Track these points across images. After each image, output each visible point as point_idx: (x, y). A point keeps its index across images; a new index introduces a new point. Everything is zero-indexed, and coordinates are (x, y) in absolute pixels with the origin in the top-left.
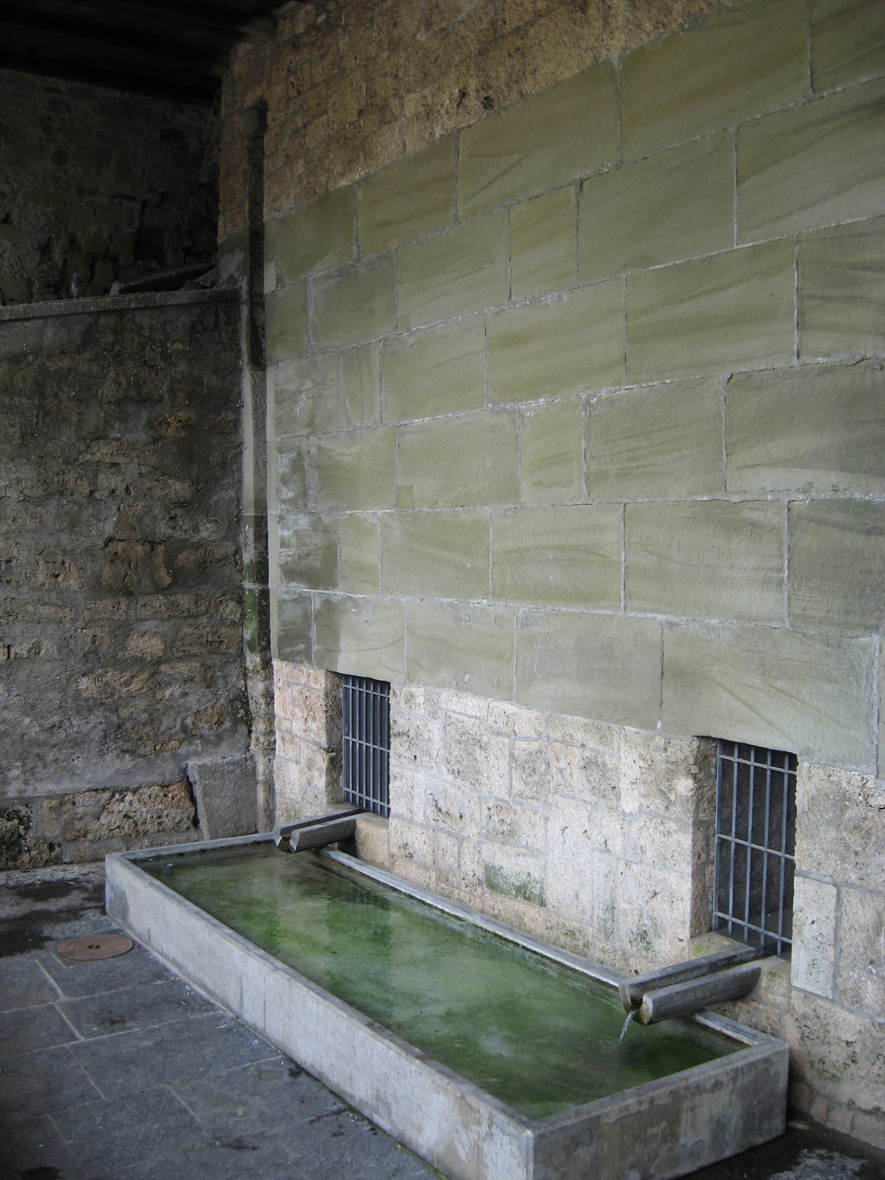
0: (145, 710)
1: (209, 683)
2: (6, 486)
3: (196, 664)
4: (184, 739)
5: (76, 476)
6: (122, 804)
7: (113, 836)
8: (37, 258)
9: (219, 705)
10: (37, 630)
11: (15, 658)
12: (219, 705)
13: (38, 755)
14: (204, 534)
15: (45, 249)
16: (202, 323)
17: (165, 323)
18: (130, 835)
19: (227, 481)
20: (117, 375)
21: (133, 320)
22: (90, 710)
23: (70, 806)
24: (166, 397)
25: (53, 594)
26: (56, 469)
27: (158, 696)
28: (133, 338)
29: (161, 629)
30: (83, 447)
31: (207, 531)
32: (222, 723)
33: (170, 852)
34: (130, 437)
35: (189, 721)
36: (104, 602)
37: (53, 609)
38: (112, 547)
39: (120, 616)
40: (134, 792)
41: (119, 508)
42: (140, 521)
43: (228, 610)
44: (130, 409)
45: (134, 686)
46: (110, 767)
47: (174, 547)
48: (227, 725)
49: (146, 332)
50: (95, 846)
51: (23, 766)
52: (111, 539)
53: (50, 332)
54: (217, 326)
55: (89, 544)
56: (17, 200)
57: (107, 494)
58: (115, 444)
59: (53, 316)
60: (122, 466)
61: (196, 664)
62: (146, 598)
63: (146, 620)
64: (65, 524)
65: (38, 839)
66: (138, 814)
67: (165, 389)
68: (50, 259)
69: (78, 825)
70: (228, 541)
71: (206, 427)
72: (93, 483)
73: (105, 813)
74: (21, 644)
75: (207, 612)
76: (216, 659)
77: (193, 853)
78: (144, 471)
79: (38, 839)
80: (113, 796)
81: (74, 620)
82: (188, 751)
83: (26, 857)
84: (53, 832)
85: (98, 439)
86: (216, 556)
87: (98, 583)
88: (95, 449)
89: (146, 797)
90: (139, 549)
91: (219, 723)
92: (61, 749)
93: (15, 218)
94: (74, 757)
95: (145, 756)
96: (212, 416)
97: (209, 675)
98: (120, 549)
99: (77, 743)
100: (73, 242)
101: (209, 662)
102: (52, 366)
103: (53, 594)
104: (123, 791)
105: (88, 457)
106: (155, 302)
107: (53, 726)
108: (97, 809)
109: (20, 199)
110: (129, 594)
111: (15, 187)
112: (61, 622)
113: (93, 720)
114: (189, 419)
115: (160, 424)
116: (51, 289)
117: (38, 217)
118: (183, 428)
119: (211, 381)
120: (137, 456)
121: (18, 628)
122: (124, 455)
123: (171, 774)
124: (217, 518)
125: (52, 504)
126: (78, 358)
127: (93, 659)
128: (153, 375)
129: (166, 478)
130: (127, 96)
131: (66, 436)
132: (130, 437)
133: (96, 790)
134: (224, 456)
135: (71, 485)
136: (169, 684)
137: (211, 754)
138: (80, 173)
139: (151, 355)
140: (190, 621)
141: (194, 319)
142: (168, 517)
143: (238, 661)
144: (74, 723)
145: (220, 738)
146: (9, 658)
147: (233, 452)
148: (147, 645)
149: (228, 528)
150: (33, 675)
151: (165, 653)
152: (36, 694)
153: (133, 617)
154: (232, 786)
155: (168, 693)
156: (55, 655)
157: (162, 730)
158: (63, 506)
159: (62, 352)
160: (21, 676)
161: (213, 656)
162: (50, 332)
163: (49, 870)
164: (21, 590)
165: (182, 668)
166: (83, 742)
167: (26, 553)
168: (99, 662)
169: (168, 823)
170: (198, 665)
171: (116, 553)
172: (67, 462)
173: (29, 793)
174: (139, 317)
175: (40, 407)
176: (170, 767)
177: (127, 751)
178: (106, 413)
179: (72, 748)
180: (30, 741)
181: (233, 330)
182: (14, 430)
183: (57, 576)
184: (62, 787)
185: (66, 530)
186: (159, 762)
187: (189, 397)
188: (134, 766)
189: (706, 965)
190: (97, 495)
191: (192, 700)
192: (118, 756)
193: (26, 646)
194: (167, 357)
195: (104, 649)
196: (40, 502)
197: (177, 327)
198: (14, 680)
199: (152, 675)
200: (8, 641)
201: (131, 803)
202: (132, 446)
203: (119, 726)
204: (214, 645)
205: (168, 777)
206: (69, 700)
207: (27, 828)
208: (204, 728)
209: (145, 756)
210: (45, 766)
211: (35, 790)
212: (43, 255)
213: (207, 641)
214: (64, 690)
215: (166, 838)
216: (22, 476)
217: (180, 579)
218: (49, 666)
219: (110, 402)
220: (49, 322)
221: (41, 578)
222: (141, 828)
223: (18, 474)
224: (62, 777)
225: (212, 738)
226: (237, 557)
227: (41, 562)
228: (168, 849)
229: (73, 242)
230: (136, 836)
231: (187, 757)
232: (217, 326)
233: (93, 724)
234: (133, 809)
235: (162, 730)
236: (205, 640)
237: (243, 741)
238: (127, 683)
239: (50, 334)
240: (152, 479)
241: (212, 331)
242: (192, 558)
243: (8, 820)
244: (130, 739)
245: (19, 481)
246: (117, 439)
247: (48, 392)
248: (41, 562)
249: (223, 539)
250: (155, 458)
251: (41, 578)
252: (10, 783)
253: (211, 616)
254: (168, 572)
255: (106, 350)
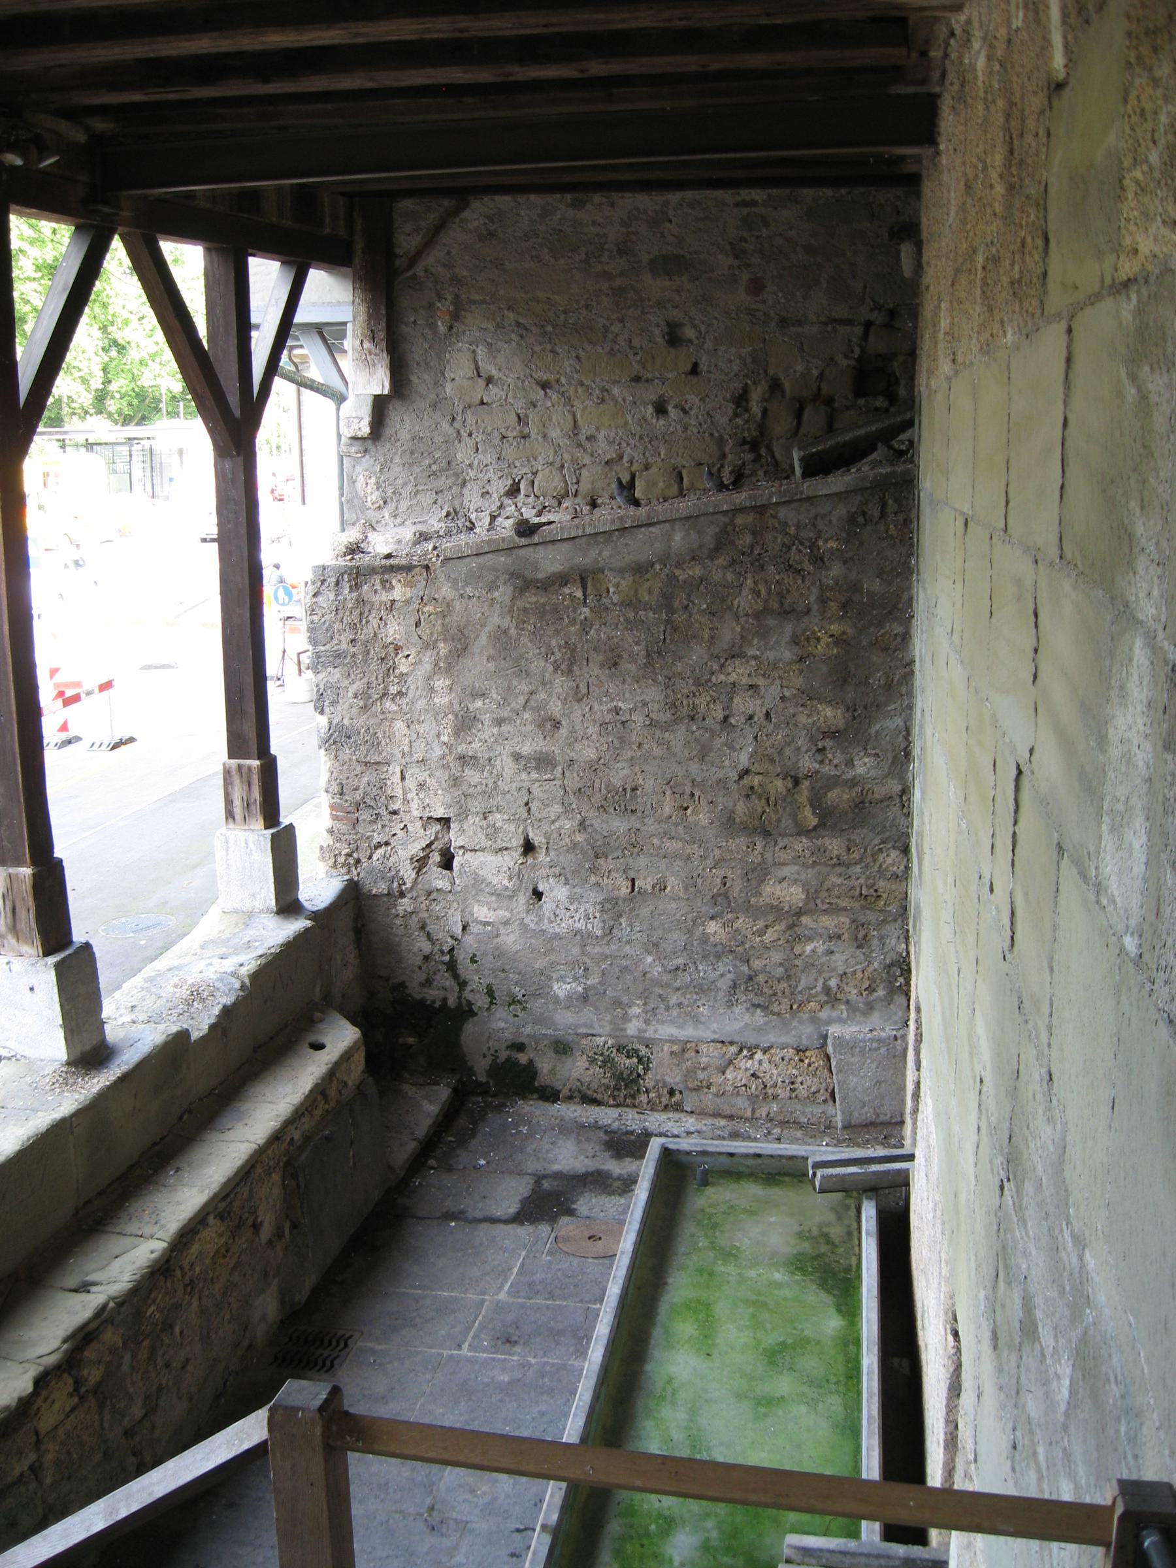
0: (781, 965)
1: (862, 943)
2: (630, 710)
3: (845, 919)
4: (827, 1002)
5: (708, 699)
6: (750, 1062)
7: (738, 1094)
8: (730, 412)
9: (871, 969)
10: (663, 864)
11: (639, 892)
12: (871, 969)
13: (660, 996)
14: (860, 770)
15: (741, 400)
16: (864, 514)
17: (816, 517)
18: (757, 1096)
19: (893, 707)
20: (755, 583)
21: (774, 517)
22: (718, 957)
23: (693, 1054)
24: (815, 607)
25: (680, 828)
26: (686, 691)
27: (797, 950)
28: (776, 538)
29: (803, 876)
30: (716, 667)
31: (864, 766)
32: (874, 990)
33: (718, 1150)
34: (771, 655)
35: (833, 983)
36: (737, 841)
37: (680, 844)
38: (746, 781)
39: (754, 857)
40: (765, 1051)
41: (756, 737)
42: (780, 752)
43: (889, 861)
44: (771, 622)
45: (769, 937)
46: (738, 1021)
47: (821, 787)
48: (881, 993)
49: (792, 530)
50: (718, 1101)
51: (645, 1004)
52: (747, 772)
53: (678, 537)
54: (883, 514)
55: (721, 776)
56: (706, 346)
57: (743, 719)
58: (753, 663)
59: (680, 519)
60: (762, 688)
61: (845, 919)
62: (786, 840)
63: (784, 864)
64: (695, 753)
65: (657, 1082)
66: (768, 1075)
67: (812, 599)
68: (747, 410)
69: (701, 1075)
70: (892, 778)
71: (864, 643)
72: (728, 707)
73: (731, 1068)
74: (645, 878)
75: (861, 860)
76: (872, 917)
77: (746, 1156)
78: (787, 694)
79: (657, 1082)
80: (741, 1050)
81: (703, 858)
82: (830, 1017)
83: (643, 1098)
84: (674, 1078)
85: (733, 657)
86: (876, 796)
87: (731, 820)
88: (730, 669)
89: (777, 1059)
90: (779, 783)
91: (871, 989)
92: (684, 994)
93: (703, 367)
94: (699, 1003)
95: (779, 1014)
96: (872, 629)
97: (861, 935)
98: (756, 783)
99: (702, 989)
100: (775, 386)
101: (862, 919)
102: (682, 575)
103: (680, 828)
104: (752, 1049)
105: (722, 677)
106: (802, 493)
107: (677, 969)
108: (722, 1062)
109: (709, 345)
110: (766, 834)
111: (703, 330)
112: (688, 858)
113: (721, 968)
114: (844, 633)
115: (808, 639)
116: (747, 447)
117: (730, 361)
118: (836, 643)
119: (873, 585)
120: (780, 677)
121: (642, 861)
122: (764, 676)
123: (809, 1038)
124: (877, 751)
125: (682, 728)
126: (710, 564)
127: (722, 900)
128: (799, 582)
129: (815, 702)
130: (843, 191)
131: (697, 654)
132: (771, 655)
133: (723, 1042)
134: (888, 677)
135: (702, 709)
136: (810, 939)
137: (858, 1023)
138: (783, 300)
139: (797, 558)
140: (839, 870)
141: (854, 510)
142: (814, 749)
143: (900, 921)
144: (700, 968)
145: (870, 1007)
146: (633, 890)
147: (901, 671)
148: (785, 892)
149: (893, 763)
150: (657, 912)
151: (806, 904)
152: (659, 933)
153: (770, 860)
154: (873, 1066)
155: (808, 948)
156: (681, 894)
157: (800, 988)
158: (693, 733)
159: (693, 558)
160: (645, 911)
161: (868, 912)
162: (678, 537)
163: (664, 1116)
164: (646, 820)
165: (827, 922)
166: (709, 989)
167: (652, 782)
168: (729, 906)
169: (802, 1091)
170: (847, 920)
171: (752, 788)
172: (697, 683)
173: (649, 1034)
174: (783, 512)
175: (668, 622)
176: (808, 1030)
177: (759, 1006)
178: (743, 628)
179: (696, 993)
180: (652, 980)
181: (905, 520)
182: (639, 648)
183: (686, 809)
184: (684, 1033)
185: (696, 760)
186: (795, 1023)
187: (844, 607)
188: (766, 1023)
189: (899, 1558)
190: (732, 720)
191: (838, 960)
192: (747, 1009)
193: (651, 881)
194: (818, 560)
195: (735, 893)
196: (667, 727)
197: (830, 521)
198: (638, 915)
199: (791, 927)
200: (632, 874)
201: (760, 1062)
202: (775, 666)
203: (750, 978)
204: (870, 899)
205: (805, 1042)
206: (695, 943)
207: (646, 1069)
208: (852, 993)
209: (779, 1014)
210: (668, 1009)
211: (656, 1031)
212: (738, 407)
213: (861, 894)
214: (690, 932)
215: (799, 1107)
216: (647, 699)
217: (828, 819)
218: (674, 905)
219: (747, 615)
220: (678, 526)
221: (667, 810)
222: (770, 1091)
223: (644, 697)
224: (685, 1023)
225: (861, 1005)
226: (904, 798)
227: (668, 793)
228: (717, 1146)
229: (775, 386)
230: (764, 1099)
231: (829, 1022)
232: (883, 514)
233: (724, 972)
234: (762, 1068)
235: (800, 988)
236: (857, 893)
237: (900, 1014)
238: (761, 933)
239: (679, 539)
240: (797, 705)
241: (877, 523)
242: (845, 797)
243: (628, 1057)
244: (762, 993)
245: (645, 704)
246: (755, 658)
247: (676, 604)
248: (668, 793)
249: (886, 776)
250: (801, 679)
251: (667, 810)
252: (630, 1021)
253: (867, 866)
254: (814, 813)
255: (743, 554)
